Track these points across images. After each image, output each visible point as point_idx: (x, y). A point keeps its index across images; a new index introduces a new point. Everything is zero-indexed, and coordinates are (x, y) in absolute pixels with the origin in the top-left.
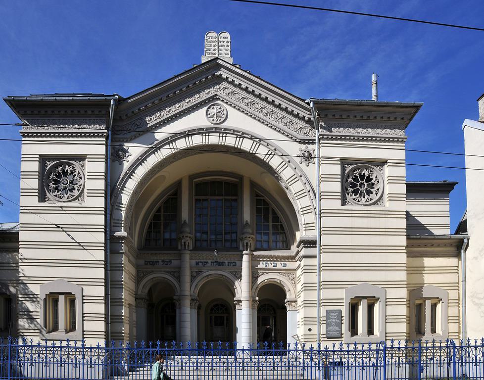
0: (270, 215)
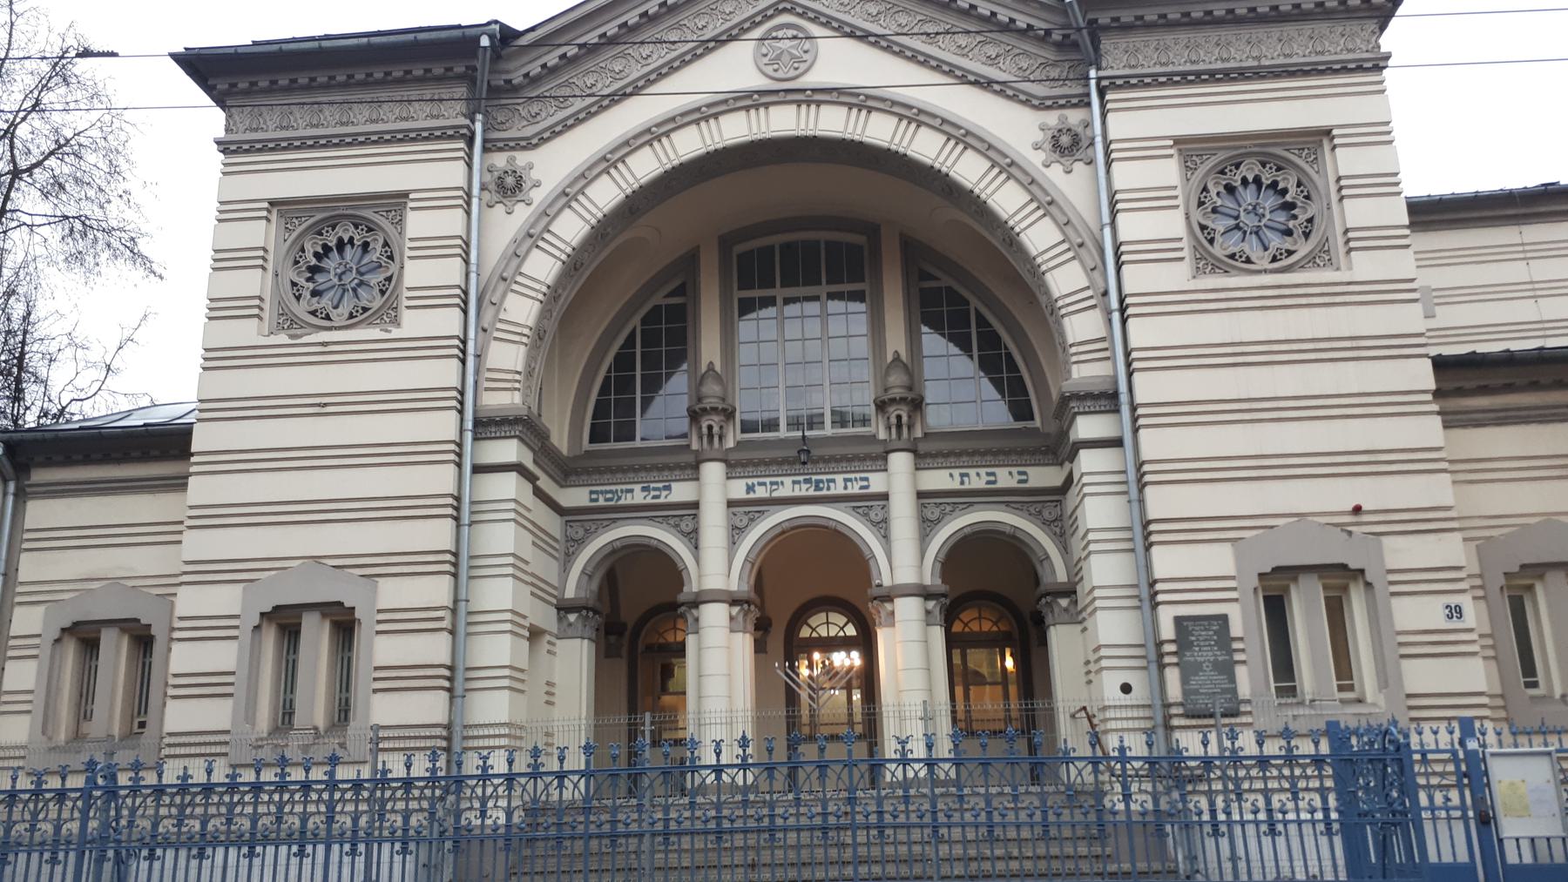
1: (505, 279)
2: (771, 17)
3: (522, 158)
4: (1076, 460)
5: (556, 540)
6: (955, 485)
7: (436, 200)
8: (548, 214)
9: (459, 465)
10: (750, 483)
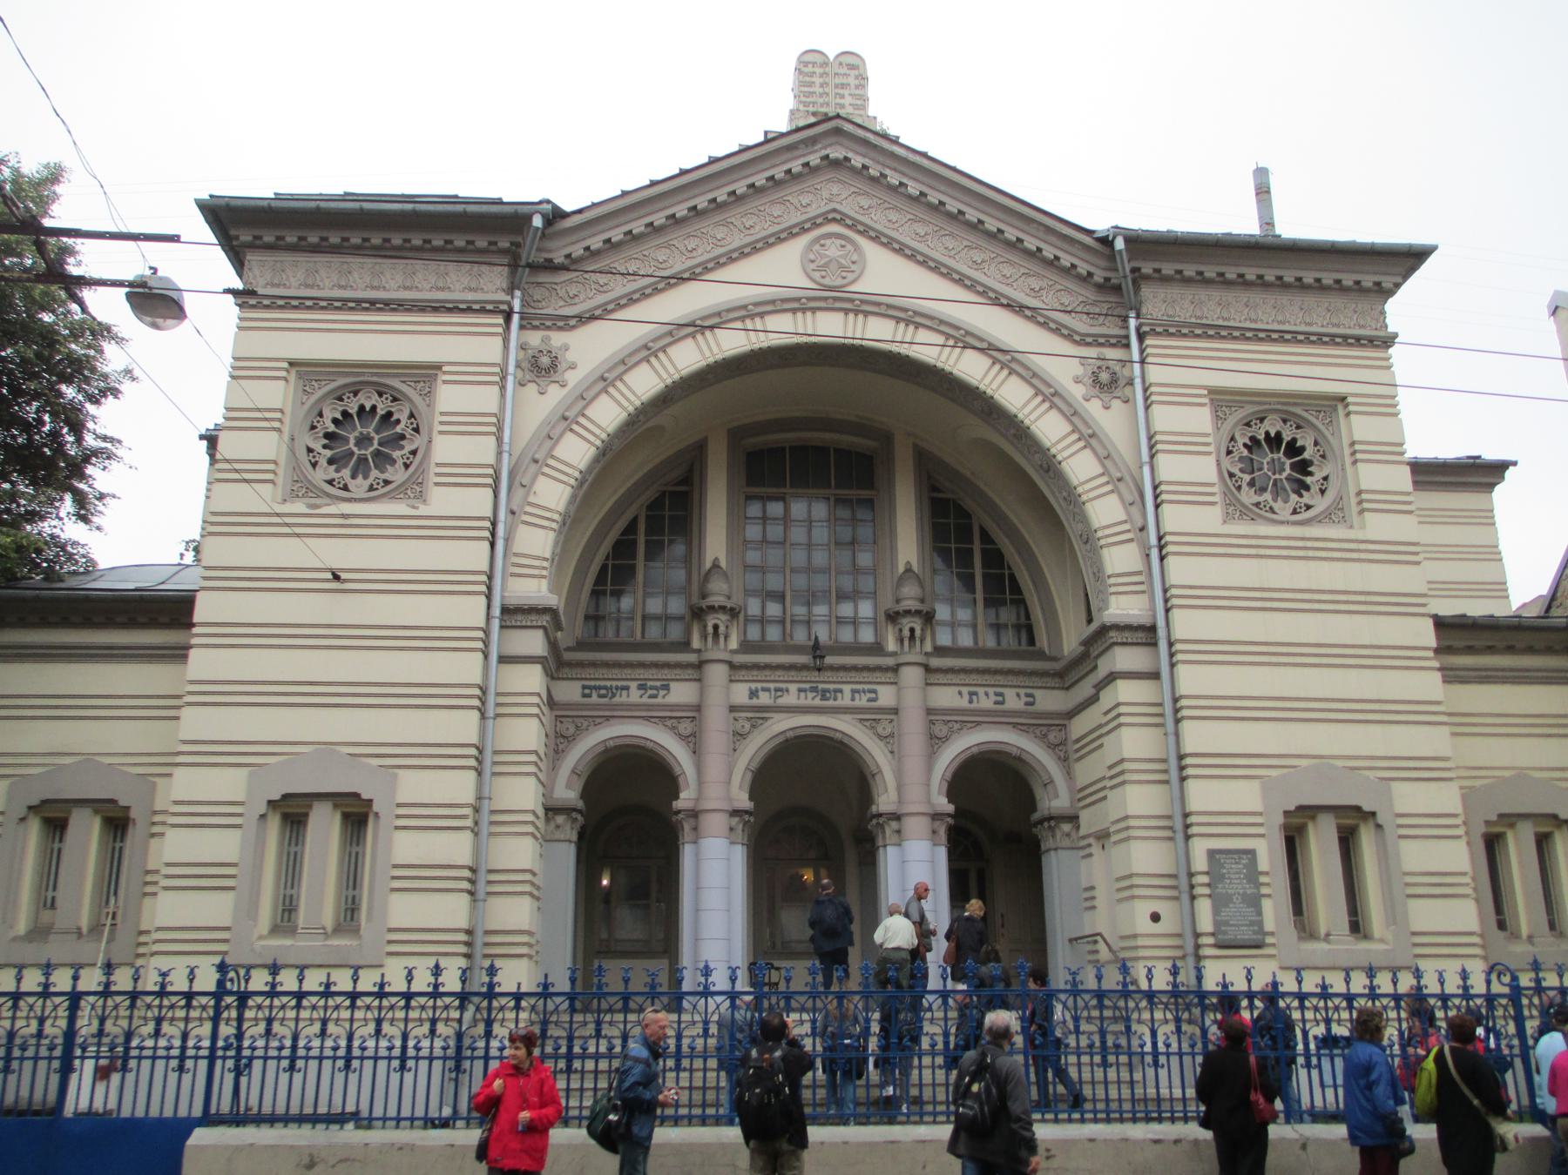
0: (977, 548)
1: (536, 461)
2: (820, 225)
3: (557, 339)
6: (963, 703)
7: (470, 374)
8: (584, 398)
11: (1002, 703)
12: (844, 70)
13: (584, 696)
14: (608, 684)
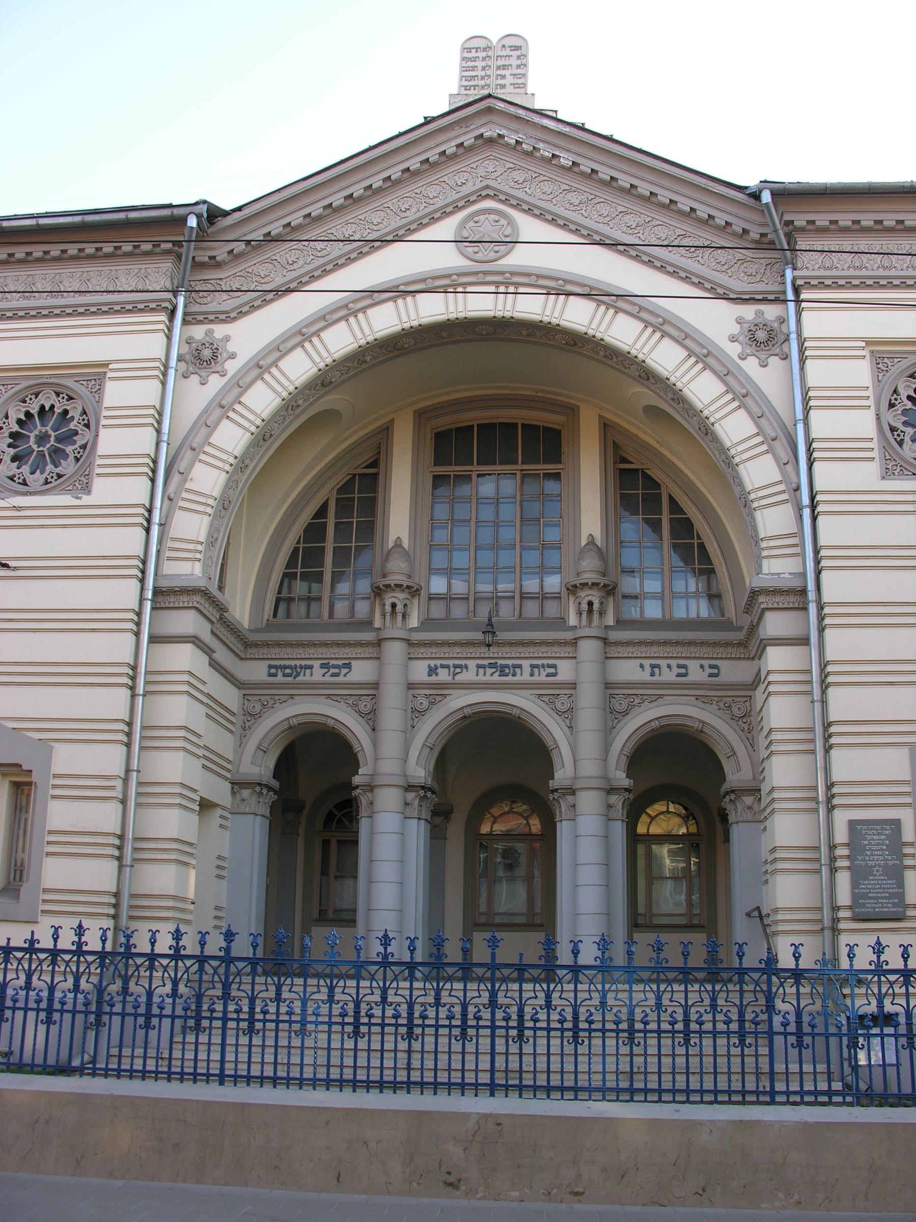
0: (665, 518)
2: (474, 202)
3: (220, 331)
4: (763, 658)
5: (233, 714)
6: (645, 676)
8: (241, 385)
9: (137, 634)
10: (432, 665)
11: (685, 675)
12: (507, 52)
13: (270, 675)
14: (293, 663)
